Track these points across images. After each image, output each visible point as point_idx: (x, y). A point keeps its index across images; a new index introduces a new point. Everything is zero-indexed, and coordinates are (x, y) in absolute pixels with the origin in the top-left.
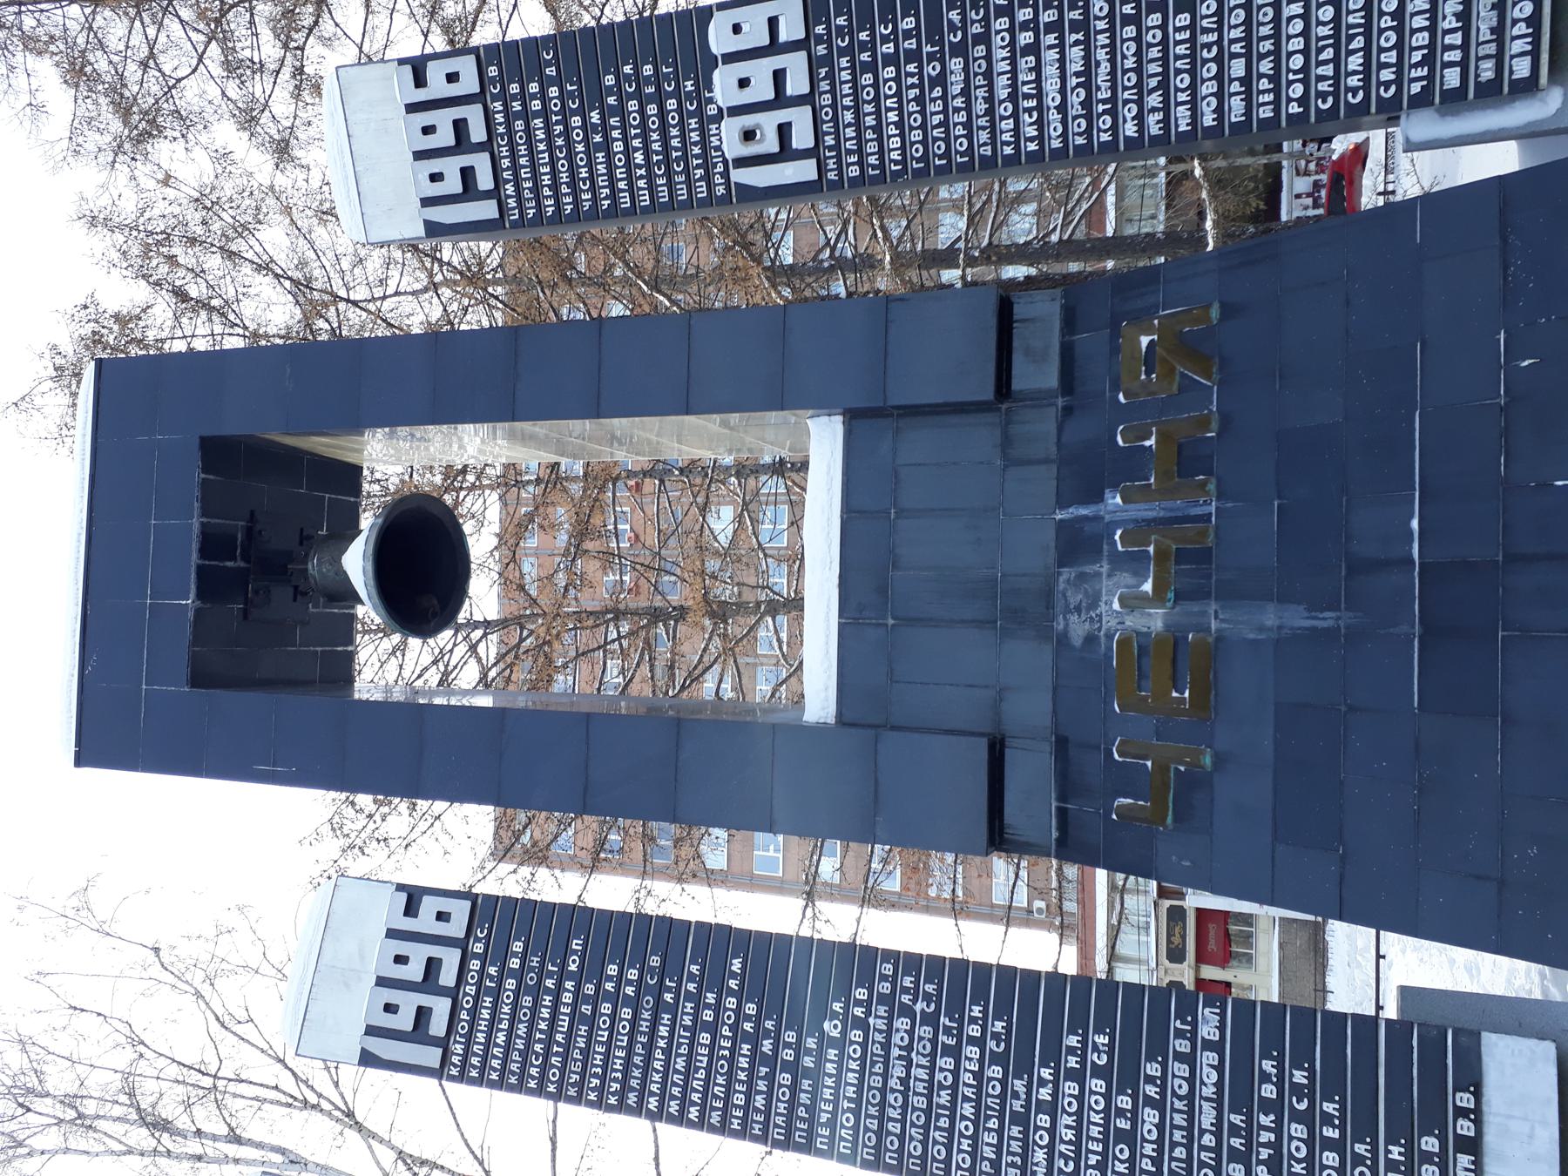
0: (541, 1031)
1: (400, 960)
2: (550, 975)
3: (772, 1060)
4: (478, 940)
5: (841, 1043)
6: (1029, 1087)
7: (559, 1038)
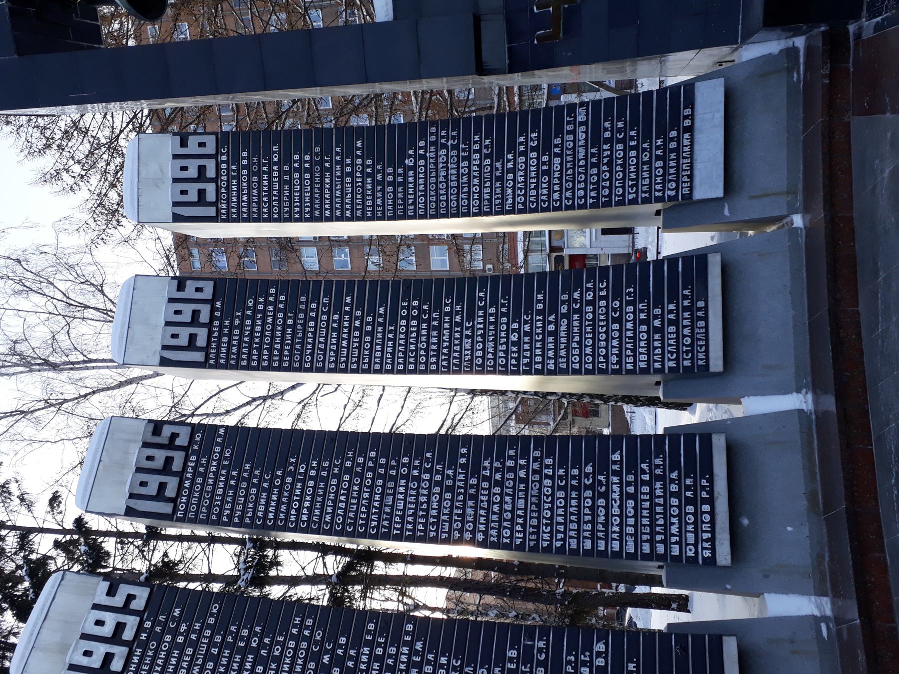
0: (265, 191)
1: (184, 169)
2: (264, 165)
3: (382, 183)
4: (223, 154)
5: (414, 168)
6: (503, 164)
7: (275, 193)
